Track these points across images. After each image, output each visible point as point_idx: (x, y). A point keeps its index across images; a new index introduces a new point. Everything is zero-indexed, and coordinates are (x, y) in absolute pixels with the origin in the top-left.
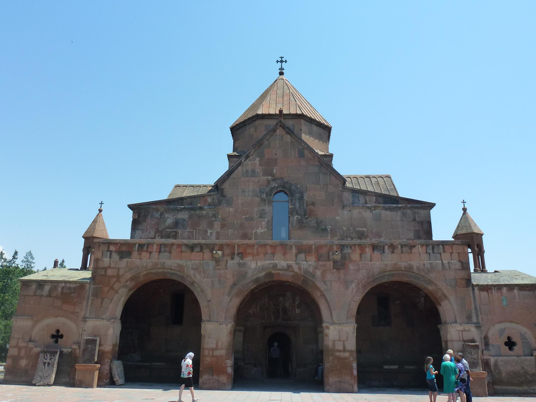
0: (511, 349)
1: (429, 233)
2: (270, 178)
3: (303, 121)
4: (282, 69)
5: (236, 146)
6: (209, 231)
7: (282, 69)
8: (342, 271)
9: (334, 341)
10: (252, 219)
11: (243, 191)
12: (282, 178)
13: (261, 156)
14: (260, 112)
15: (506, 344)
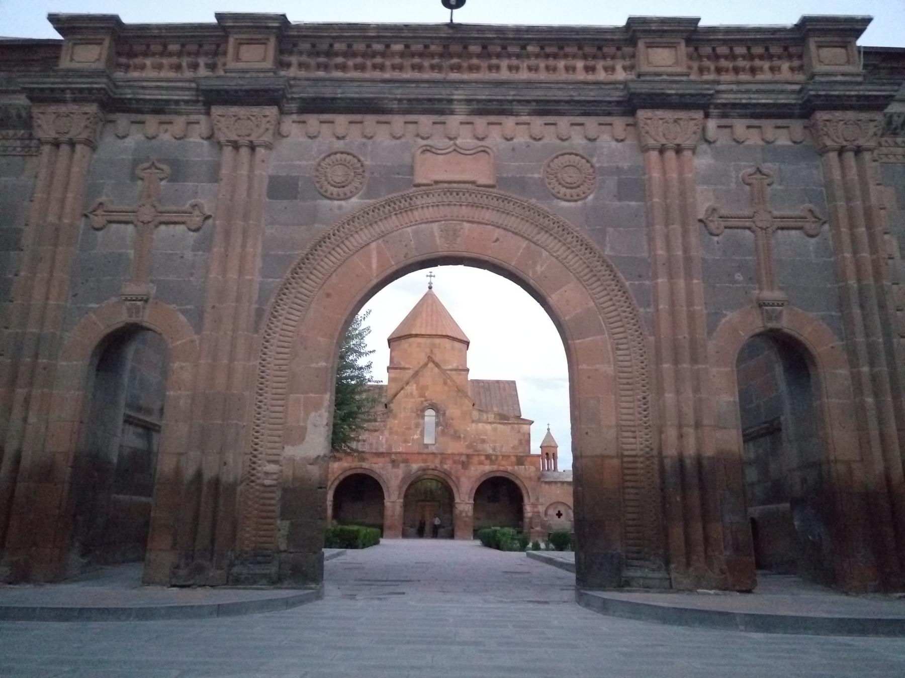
0: (559, 517)
1: (528, 441)
2: (423, 399)
3: (446, 340)
4: (430, 283)
5: (393, 355)
6: (381, 437)
7: (430, 283)
8: (467, 471)
9: (461, 512)
10: (409, 429)
11: (405, 408)
12: (431, 400)
13: (418, 384)
14: (414, 333)
15: (557, 515)
